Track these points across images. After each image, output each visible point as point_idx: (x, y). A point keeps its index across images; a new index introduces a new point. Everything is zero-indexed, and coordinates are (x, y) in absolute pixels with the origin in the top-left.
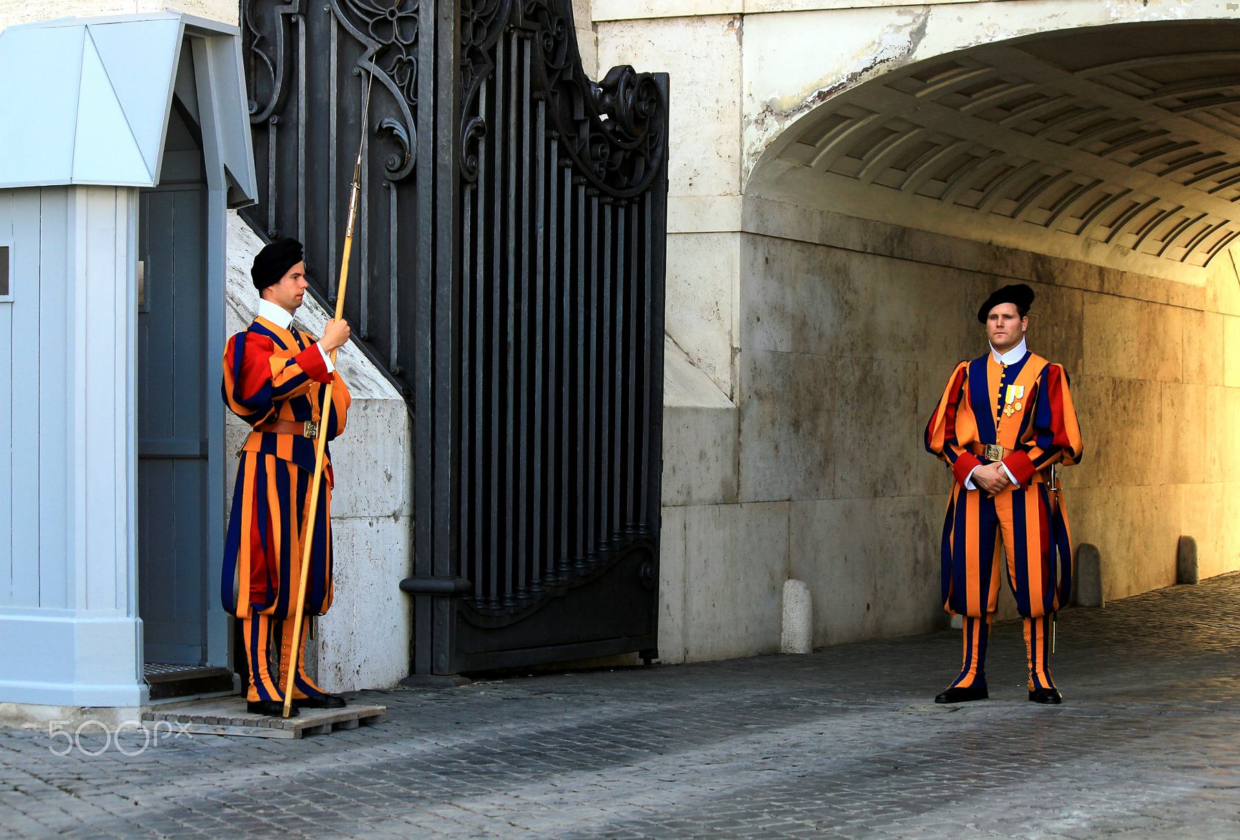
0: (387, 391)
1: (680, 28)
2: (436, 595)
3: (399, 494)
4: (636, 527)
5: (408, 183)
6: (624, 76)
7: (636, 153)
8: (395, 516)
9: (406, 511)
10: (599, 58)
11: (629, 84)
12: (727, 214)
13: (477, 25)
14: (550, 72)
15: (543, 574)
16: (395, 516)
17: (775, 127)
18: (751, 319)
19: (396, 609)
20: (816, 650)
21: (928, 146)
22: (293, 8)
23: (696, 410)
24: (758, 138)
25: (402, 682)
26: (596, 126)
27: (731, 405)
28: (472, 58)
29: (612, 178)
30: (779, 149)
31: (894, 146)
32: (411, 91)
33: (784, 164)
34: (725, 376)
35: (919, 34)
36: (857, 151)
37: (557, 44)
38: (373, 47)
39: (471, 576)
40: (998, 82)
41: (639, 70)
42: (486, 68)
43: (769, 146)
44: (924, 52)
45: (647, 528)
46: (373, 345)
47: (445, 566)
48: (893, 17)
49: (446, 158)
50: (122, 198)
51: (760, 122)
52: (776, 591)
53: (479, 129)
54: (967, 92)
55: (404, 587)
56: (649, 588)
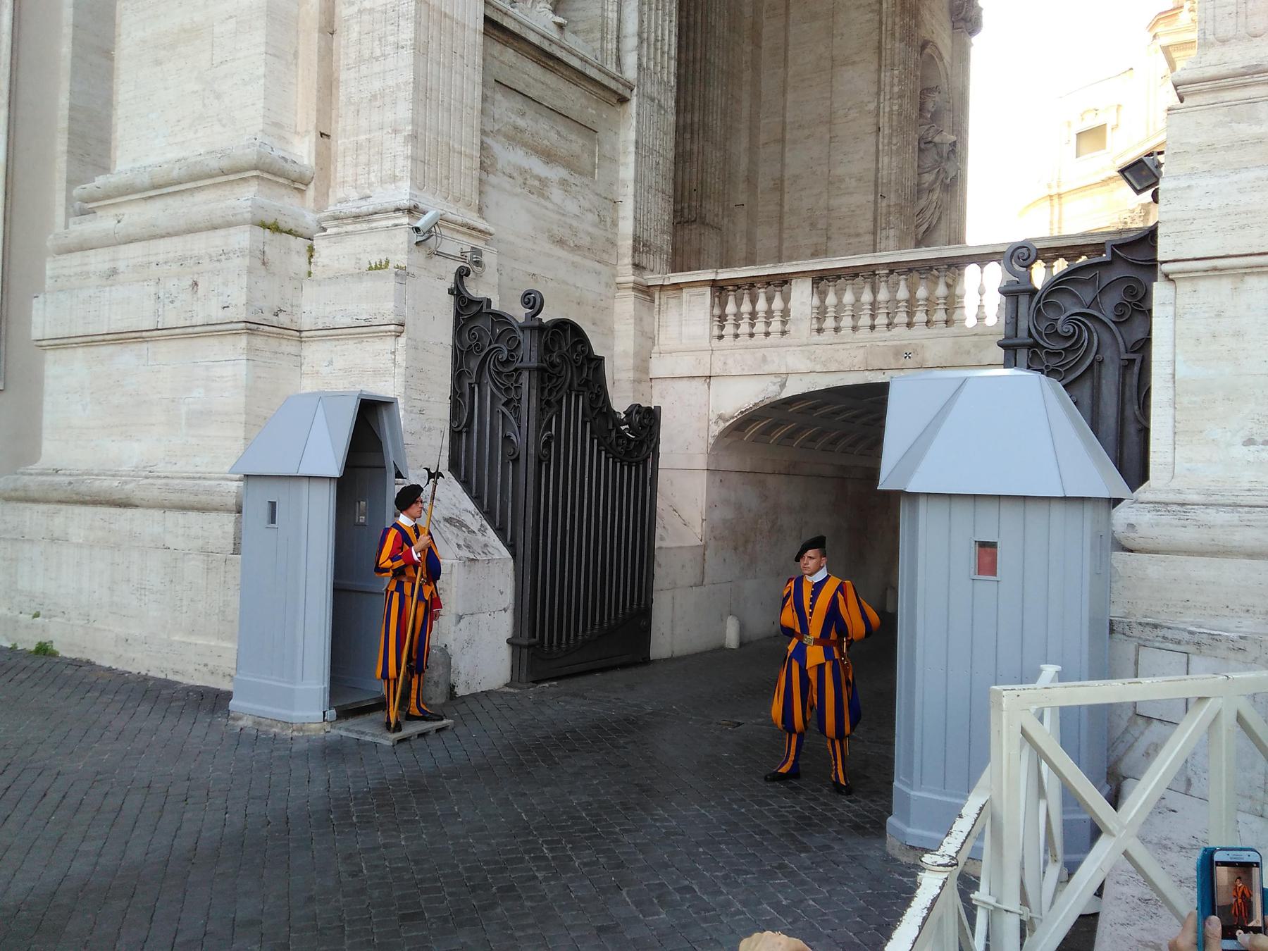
0: (506, 553)
1: (685, 382)
2: (521, 647)
3: (508, 599)
4: (639, 604)
5: (516, 461)
6: (636, 410)
7: (641, 443)
8: (505, 610)
9: (512, 607)
10: (620, 403)
11: (637, 412)
12: (701, 462)
13: (550, 391)
14: (593, 409)
15: (584, 630)
16: (505, 610)
17: (722, 425)
18: (711, 506)
19: (505, 653)
20: (741, 644)
21: (798, 430)
22: (473, 381)
23: (680, 547)
24: (716, 429)
25: (506, 685)
26: (619, 431)
27: (700, 543)
28: (545, 405)
29: (628, 453)
30: (726, 433)
31: (778, 434)
32: (518, 419)
33: (728, 440)
34: (698, 530)
35: (783, 386)
36: (767, 432)
37: (598, 396)
38: (504, 400)
39: (542, 637)
40: (827, 404)
41: (644, 405)
42: (554, 409)
43: (721, 433)
44: (785, 395)
45: (646, 604)
46: (500, 531)
47: (526, 634)
48: (772, 378)
49: (532, 451)
50: (327, 484)
51: (716, 423)
52: (722, 620)
53: (550, 437)
54: (815, 408)
55: (508, 641)
56: (647, 630)
